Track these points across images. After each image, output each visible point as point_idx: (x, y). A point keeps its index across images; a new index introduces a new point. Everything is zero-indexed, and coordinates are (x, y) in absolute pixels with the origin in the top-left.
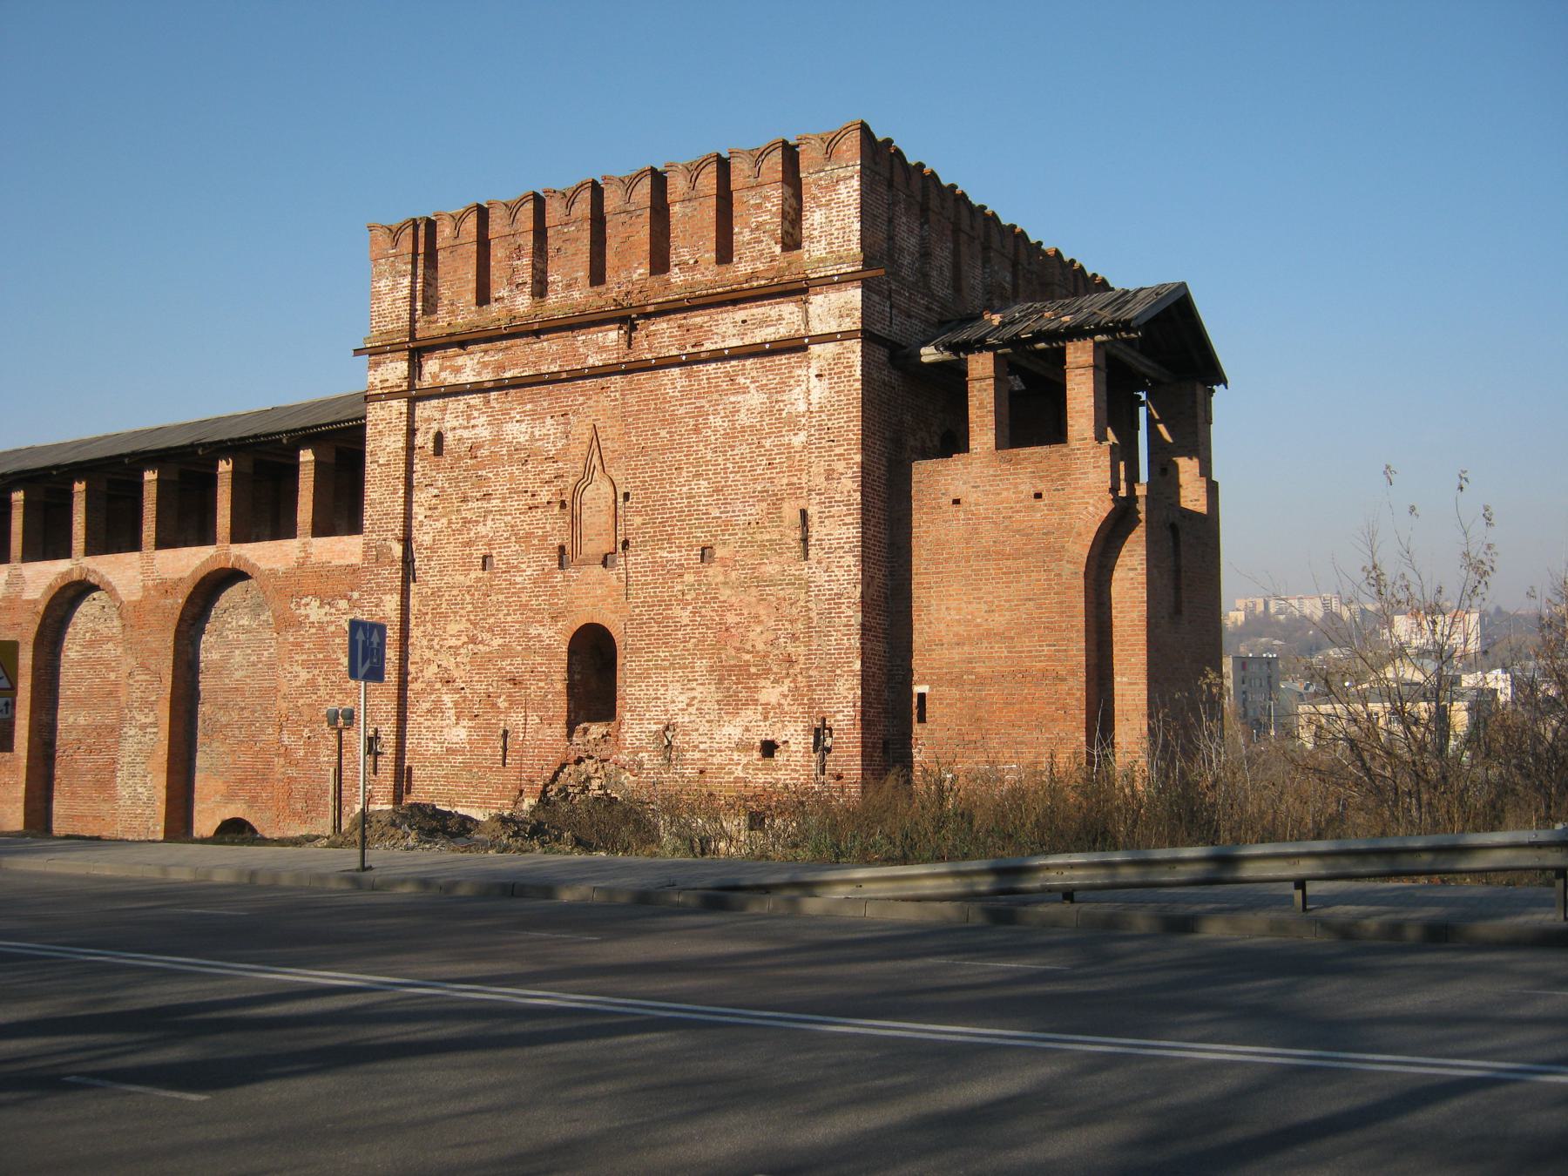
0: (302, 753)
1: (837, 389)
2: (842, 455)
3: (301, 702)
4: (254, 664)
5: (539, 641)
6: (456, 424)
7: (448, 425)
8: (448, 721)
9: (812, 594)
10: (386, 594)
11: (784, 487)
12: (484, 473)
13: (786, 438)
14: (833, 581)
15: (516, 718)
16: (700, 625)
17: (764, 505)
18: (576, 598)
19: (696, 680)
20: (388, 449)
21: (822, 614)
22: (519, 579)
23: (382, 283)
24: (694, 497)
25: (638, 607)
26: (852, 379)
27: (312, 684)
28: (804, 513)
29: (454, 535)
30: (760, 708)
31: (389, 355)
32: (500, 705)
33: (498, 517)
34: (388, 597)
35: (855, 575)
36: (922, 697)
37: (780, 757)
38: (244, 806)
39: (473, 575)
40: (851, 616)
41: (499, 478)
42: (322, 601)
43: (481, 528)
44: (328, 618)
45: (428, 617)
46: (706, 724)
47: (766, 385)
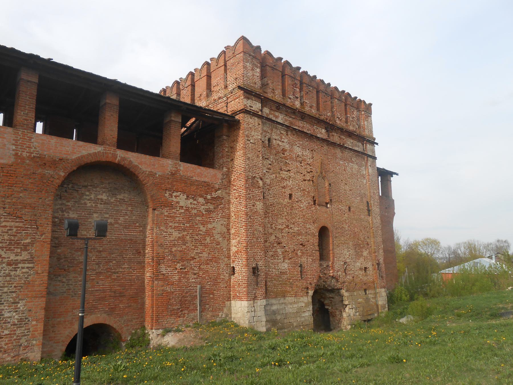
0: (177, 278)
3: (174, 249)
6: (277, 138)
10: (257, 201)
15: (304, 259)
18: (320, 216)
20: (254, 137)
22: (302, 206)
23: (248, 64)
25: (335, 222)
27: (182, 239)
28: (367, 202)
29: (278, 183)
31: (252, 97)
32: (299, 254)
34: (258, 203)
38: (104, 315)
39: (286, 200)
41: (293, 165)
42: (187, 196)
44: (193, 206)
45: (270, 215)
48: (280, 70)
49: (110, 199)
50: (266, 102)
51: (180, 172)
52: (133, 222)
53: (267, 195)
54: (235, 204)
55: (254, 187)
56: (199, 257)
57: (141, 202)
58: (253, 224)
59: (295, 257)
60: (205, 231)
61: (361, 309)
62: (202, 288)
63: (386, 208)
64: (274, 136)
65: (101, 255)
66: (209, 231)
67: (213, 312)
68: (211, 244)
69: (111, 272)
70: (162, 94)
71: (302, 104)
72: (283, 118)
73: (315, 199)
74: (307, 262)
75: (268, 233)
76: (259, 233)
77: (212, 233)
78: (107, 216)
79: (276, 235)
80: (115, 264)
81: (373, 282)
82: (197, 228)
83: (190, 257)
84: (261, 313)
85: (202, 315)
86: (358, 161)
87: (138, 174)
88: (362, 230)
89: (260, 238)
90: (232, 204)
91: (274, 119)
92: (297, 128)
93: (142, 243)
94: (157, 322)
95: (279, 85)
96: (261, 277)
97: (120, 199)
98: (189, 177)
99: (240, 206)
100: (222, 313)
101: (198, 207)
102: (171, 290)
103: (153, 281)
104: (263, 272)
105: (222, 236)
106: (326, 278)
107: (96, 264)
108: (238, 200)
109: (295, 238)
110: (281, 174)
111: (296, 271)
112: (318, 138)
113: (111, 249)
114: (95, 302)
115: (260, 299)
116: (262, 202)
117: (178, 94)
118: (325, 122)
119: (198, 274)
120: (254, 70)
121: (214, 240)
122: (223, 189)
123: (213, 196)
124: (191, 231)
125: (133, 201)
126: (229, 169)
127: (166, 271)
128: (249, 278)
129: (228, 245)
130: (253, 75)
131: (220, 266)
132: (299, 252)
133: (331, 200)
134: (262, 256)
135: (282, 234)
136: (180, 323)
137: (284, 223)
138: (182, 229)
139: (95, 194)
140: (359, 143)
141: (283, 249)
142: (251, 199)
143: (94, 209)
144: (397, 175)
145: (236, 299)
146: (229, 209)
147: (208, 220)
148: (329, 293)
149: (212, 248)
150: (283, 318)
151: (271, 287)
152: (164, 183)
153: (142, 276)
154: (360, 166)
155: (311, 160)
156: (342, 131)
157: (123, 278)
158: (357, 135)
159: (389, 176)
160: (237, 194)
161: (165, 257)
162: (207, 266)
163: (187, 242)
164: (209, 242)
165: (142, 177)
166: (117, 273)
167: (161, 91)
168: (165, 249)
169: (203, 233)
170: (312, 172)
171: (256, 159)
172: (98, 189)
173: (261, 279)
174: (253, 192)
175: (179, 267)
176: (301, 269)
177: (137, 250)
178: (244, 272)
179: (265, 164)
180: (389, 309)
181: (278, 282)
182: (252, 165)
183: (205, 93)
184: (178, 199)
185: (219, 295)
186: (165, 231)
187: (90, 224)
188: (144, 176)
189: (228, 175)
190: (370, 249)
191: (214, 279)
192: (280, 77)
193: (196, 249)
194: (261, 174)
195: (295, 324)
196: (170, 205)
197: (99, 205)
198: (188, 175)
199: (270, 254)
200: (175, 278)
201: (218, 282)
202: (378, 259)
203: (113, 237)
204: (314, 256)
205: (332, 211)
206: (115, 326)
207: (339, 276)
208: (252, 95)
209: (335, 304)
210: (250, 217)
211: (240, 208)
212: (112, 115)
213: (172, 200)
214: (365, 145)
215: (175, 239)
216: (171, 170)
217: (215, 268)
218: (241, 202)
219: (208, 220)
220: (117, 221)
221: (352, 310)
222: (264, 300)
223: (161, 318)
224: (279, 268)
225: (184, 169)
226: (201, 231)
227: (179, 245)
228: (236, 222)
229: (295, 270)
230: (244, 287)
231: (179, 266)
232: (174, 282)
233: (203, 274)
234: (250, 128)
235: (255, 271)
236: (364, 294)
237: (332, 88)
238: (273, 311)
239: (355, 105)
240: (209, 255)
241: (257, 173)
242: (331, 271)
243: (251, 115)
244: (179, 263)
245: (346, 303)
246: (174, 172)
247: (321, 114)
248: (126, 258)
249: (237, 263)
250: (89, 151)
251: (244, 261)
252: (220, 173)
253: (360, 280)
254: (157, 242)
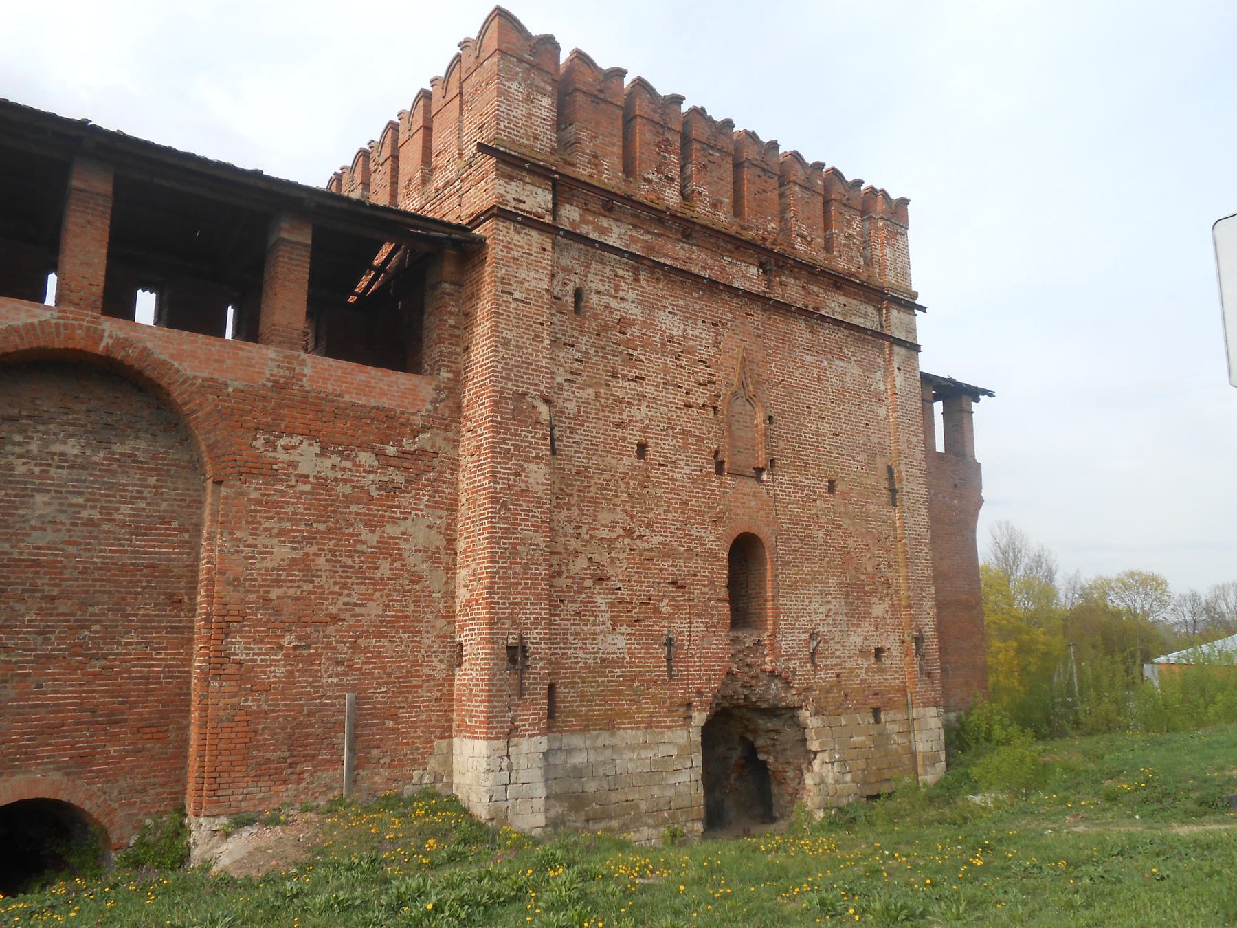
0: (280, 672)
3: (275, 593)
4: (90, 523)
5: (701, 544)
6: (602, 288)
8: (602, 627)
10: (530, 462)
12: (635, 353)
15: (680, 625)
18: (734, 506)
20: (526, 285)
22: (677, 476)
23: (514, 85)
25: (785, 523)
27: (305, 566)
29: (604, 411)
31: (525, 174)
32: (663, 610)
34: (533, 467)
37: (887, 662)
38: (57, 776)
39: (626, 461)
41: (653, 365)
42: (324, 448)
43: (634, 410)
44: (339, 475)
45: (574, 500)
48: (619, 103)
49: (88, 453)
50: (570, 188)
51: (301, 380)
52: (160, 517)
53: (565, 446)
54: (468, 471)
55: (520, 421)
56: (353, 616)
57: (189, 462)
58: (515, 524)
59: (651, 617)
60: (374, 544)
61: (861, 763)
62: (358, 701)
63: (955, 486)
64: (593, 283)
65: (55, 608)
66: (388, 543)
67: (395, 767)
68: (395, 579)
69: (86, 656)
70: (334, 190)
71: (685, 196)
72: (625, 234)
73: (720, 457)
74: (690, 631)
75: (567, 549)
76: (533, 550)
77: (399, 549)
78: (80, 501)
79: (590, 556)
80: (96, 632)
81: (903, 690)
82: (352, 535)
83: (327, 615)
84: (531, 775)
85: (359, 777)
86: (860, 356)
87: (169, 384)
88: (871, 546)
89: (537, 564)
90: (463, 471)
91: (594, 235)
92: (668, 262)
93: (185, 576)
94: (213, 798)
95: (614, 145)
96: (534, 674)
97: (121, 454)
98: (332, 394)
99: (479, 475)
100: (421, 772)
101: (356, 479)
102: (259, 706)
103: (206, 680)
104: (541, 659)
105: (431, 557)
106: (752, 678)
107: (36, 633)
108: (475, 458)
109: (655, 564)
110: (614, 386)
111: (654, 658)
112: (733, 291)
113: (87, 592)
114: (28, 740)
115: (530, 736)
116: (546, 465)
117: (366, 185)
118: (759, 246)
119: (351, 663)
120: (532, 102)
121: (402, 570)
122: (438, 429)
123: (406, 447)
124: (332, 543)
125: (164, 459)
126: (457, 373)
127: (248, 655)
128: (494, 675)
129: (446, 583)
130: (530, 115)
131: (419, 642)
132: (664, 604)
133: (772, 461)
134: (540, 614)
135: (612, 555)
136: (288, 800)
137: (618, 523)
138: (303, 537)
139: (41, 439)
140: (867, 306)
141: (614, 597)
142: (510, 455)
143: (37, 481)
144: (991, 395)
145: (463, 734)
146: (454, 484)
147: (387, 514)
148: (765, 717)
149: (395, 590)
150: (607, 787)
151: (569, 702)
152: (251, 411)
153: (184, 666)
154: (869, 369)
155: (712, 351)
156: (811, 272)
157: (118, 673)
158: (861, 285)
159: (965, 398)
160: (474, 443)
161: (247, 614)
162: (380, 641)
163: (319, 573)
164: (388, 574)
165: (181, 394)
166: (105, 657)
167: (330, 184)
168: (247, 591)
169: (370, 550)
170: (714, 383)
171: (530, 344)
172: (51, 426)
173: (534, 679)
174: (516, 435)
175: (290, 643)
176: (669, 651)
177: (170, 596)
178: (482, 659)
179: (563, 360)
180: (948, 765)
181: (592, 687)
182: (516, 361)
183: (418, 174)
184: (294, 456)
185: (412, 722)
186: (250, 541)
187: (24, 522)
188: (186, 391)
189: (454, 389)
190: (895, 598)
191: (401, 677)
192: (619, 123)
193: (346, 592)
194: (546, 387)
195: (644, 806)
196: (269, 473)
197: (52, 471)
198: (326, 388)
199: (571, 609)
200: (275, 672)
201: (413, 686)
202: (916, 625)
203: (95, 560)
204: (713, 616)
205: (775, 490)
206: (87, 806)
207: (794, 672)
208: (526, 169)
209: (785, 750)
210: (506, 506)
211: (480, 481)
212: (88, 222)
213: (274, 458)
214: (884, 311)
215: (279, 565)
216: (272, 375)
217: (403, 647)
218: (482, 465)
219: (387, 514)
220: (111, 514)
221: (830, 765)
222: (544, 739)
223: (226, 786)
224: (599, 649)
225: (314, 372)
226: (364, 543)
227: (291, 581)
228: (469, 518)
229: (651, 653)
230: (482, 701)
231: (288, 640)
232: (270, 684)
233: (364, 663)
234: (514, 258)
235: (516, 655)
236: (872, 721)
237: (785, 155)
238: (575, 768)
239: (856, 203)
240: (385, 611)
241: (531, 384)
242: (768, 659)
243: (519, 223)
244: (289, 631)
245: (814, 746)
246: (282, 381)
247: (746, 225)
248: (135, 615)
249: (468, 633)
250: (13, 320)
251: (483, 629)
252: (430, 384)
253: (861, 684)
254: (224, 574)
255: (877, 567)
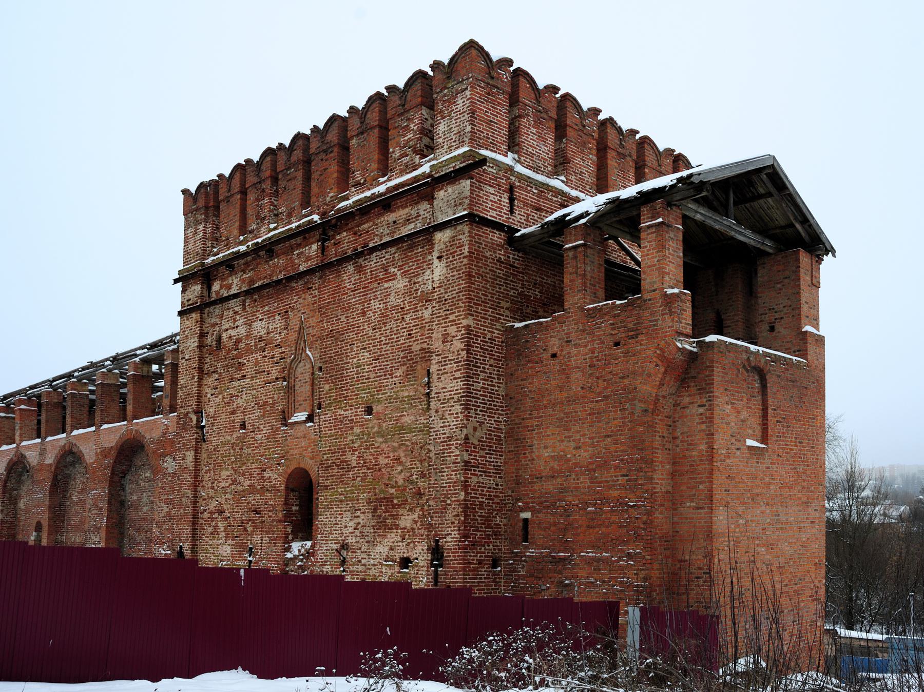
1: (452, 267)
2: (454, 321)
6: (227, 326)
7: (224, 327)
9: (431, 438)
11: (418, 353)
13: (420, 312)
14: (446, 426)
16: (363, 466)
17: (405, 368)
19: (360, 510)
21: (438, 454)
24: (360, 366)
25: (325, 454)
26: (462, 256)
30: (399, 531)
32: (248, 529)
33: (249, 392)
35: (461, 420)
36: (526, 521)
40: (457, 455)
41: (249, 361)
43: (239, 400)
46: (366, 544)
47: (408, 271)
88: (403, 459)
132: (248, 525)
205: (320, 428)
255: (408, 480)
